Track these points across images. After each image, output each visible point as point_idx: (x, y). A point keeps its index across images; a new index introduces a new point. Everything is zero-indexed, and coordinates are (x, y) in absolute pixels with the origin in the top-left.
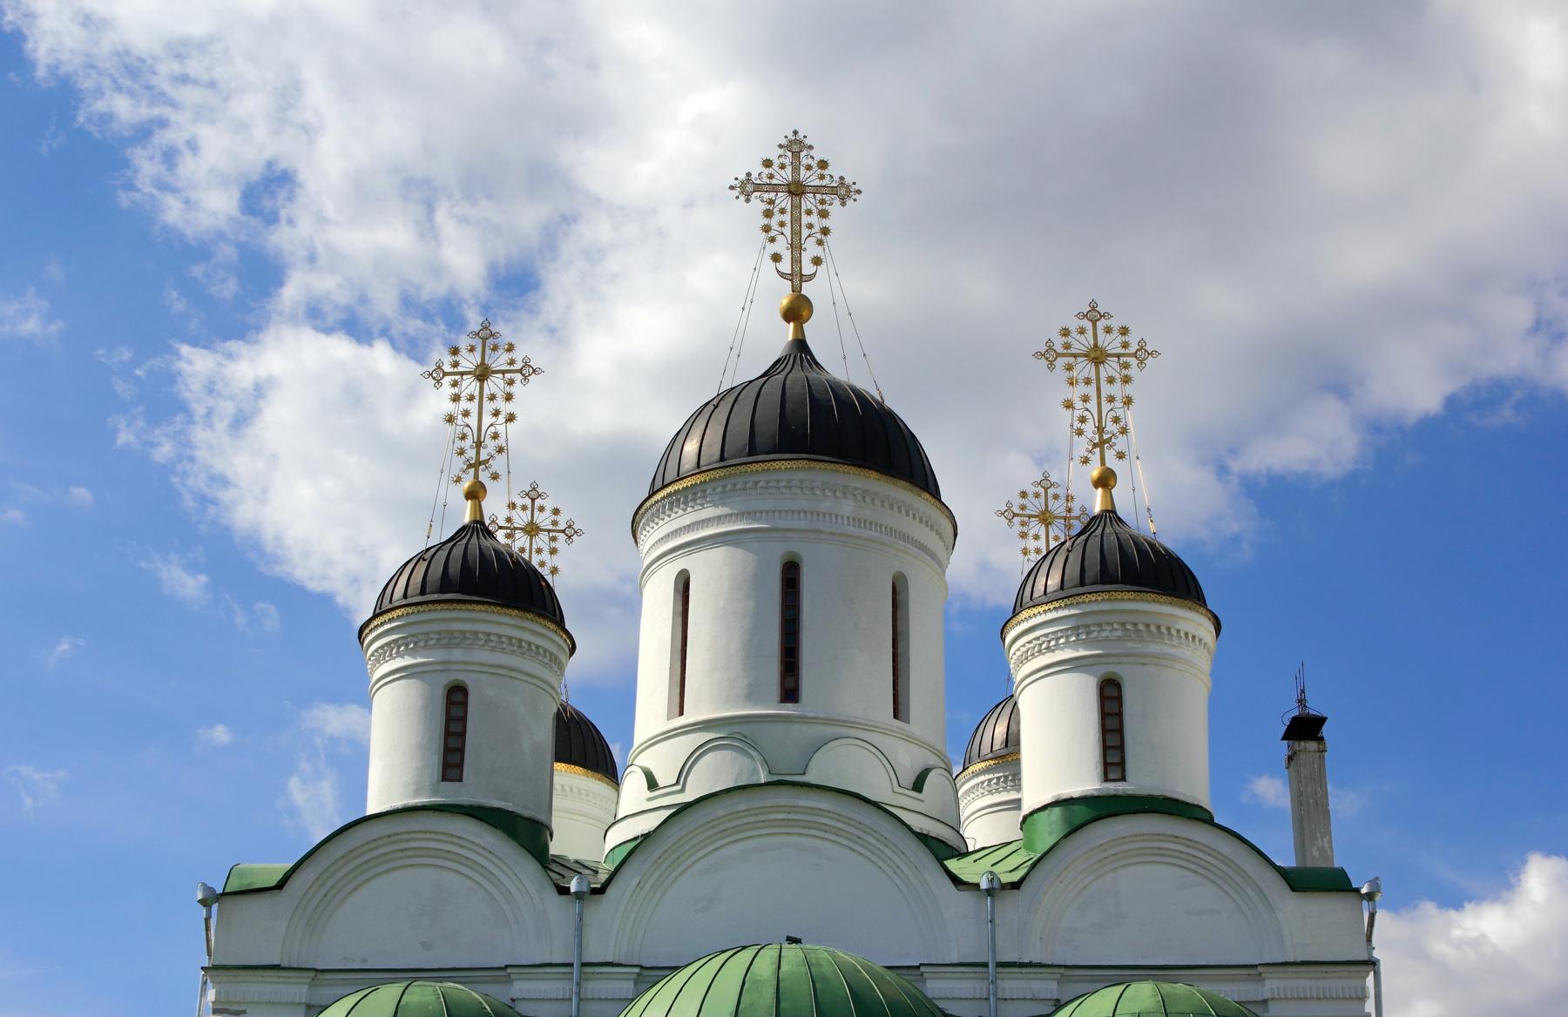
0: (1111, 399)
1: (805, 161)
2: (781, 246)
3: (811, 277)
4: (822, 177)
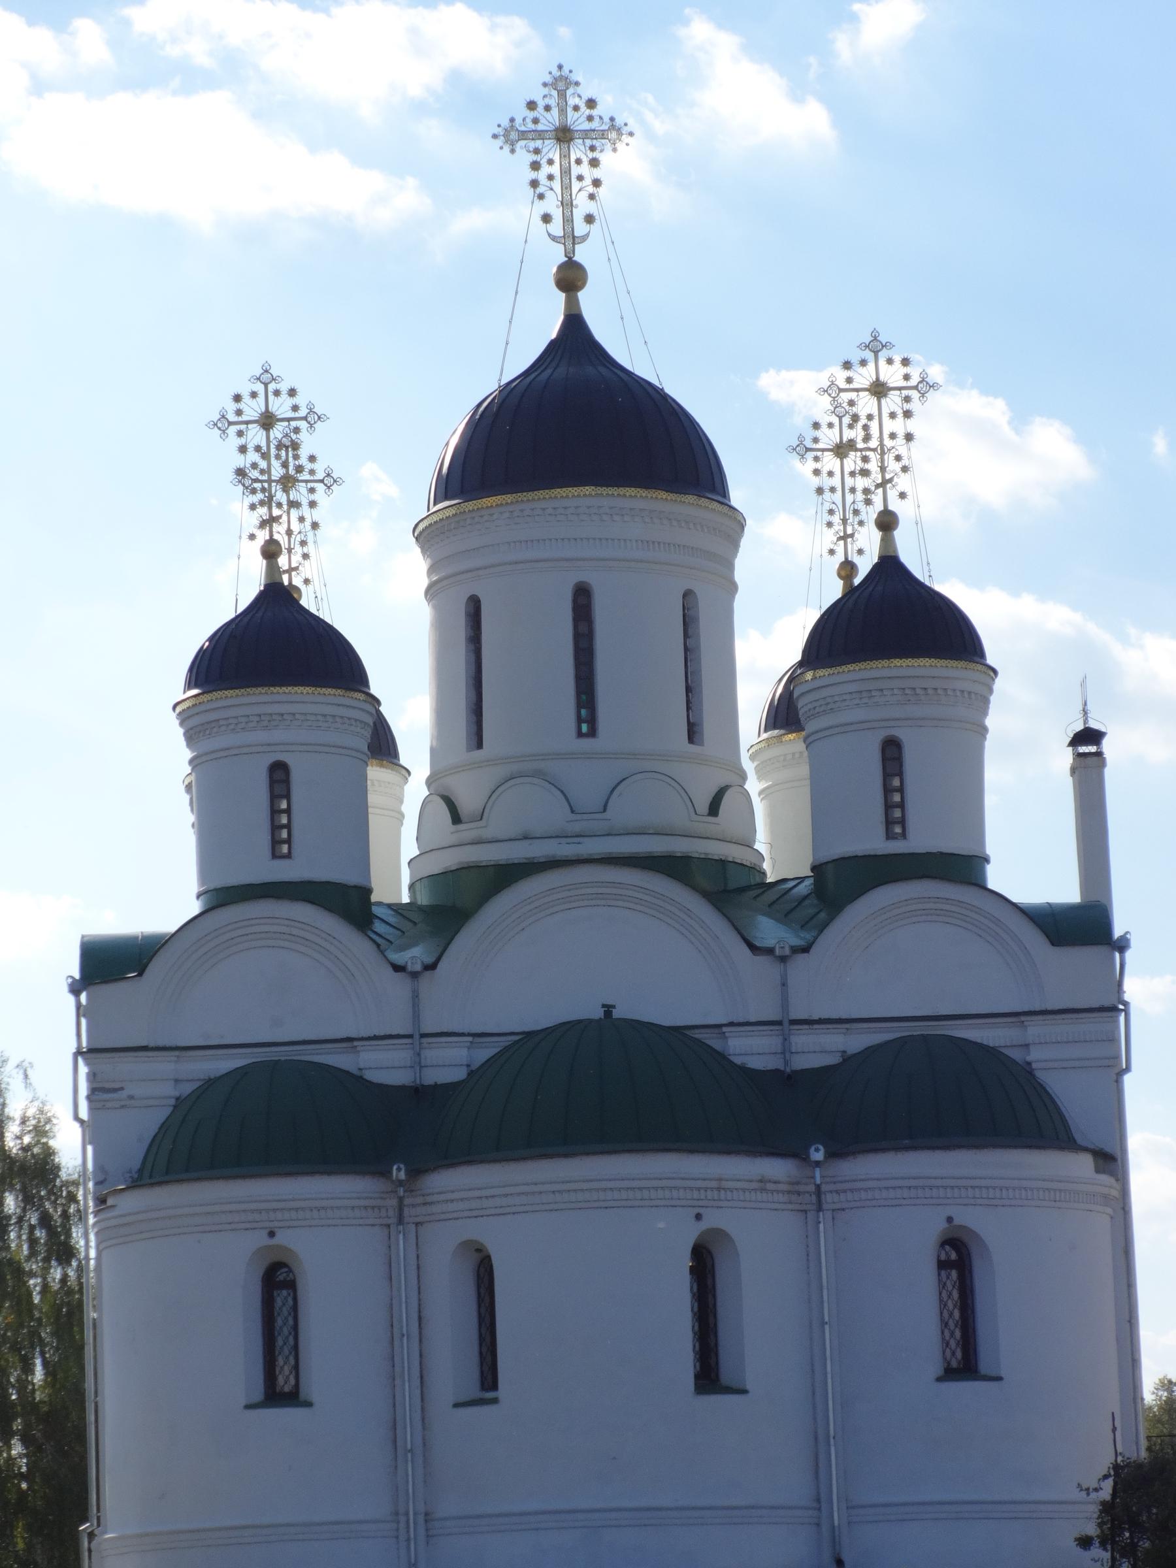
0: (893, 436)
1: (572, 101)
2: (552, 205)
3: (584, 238)
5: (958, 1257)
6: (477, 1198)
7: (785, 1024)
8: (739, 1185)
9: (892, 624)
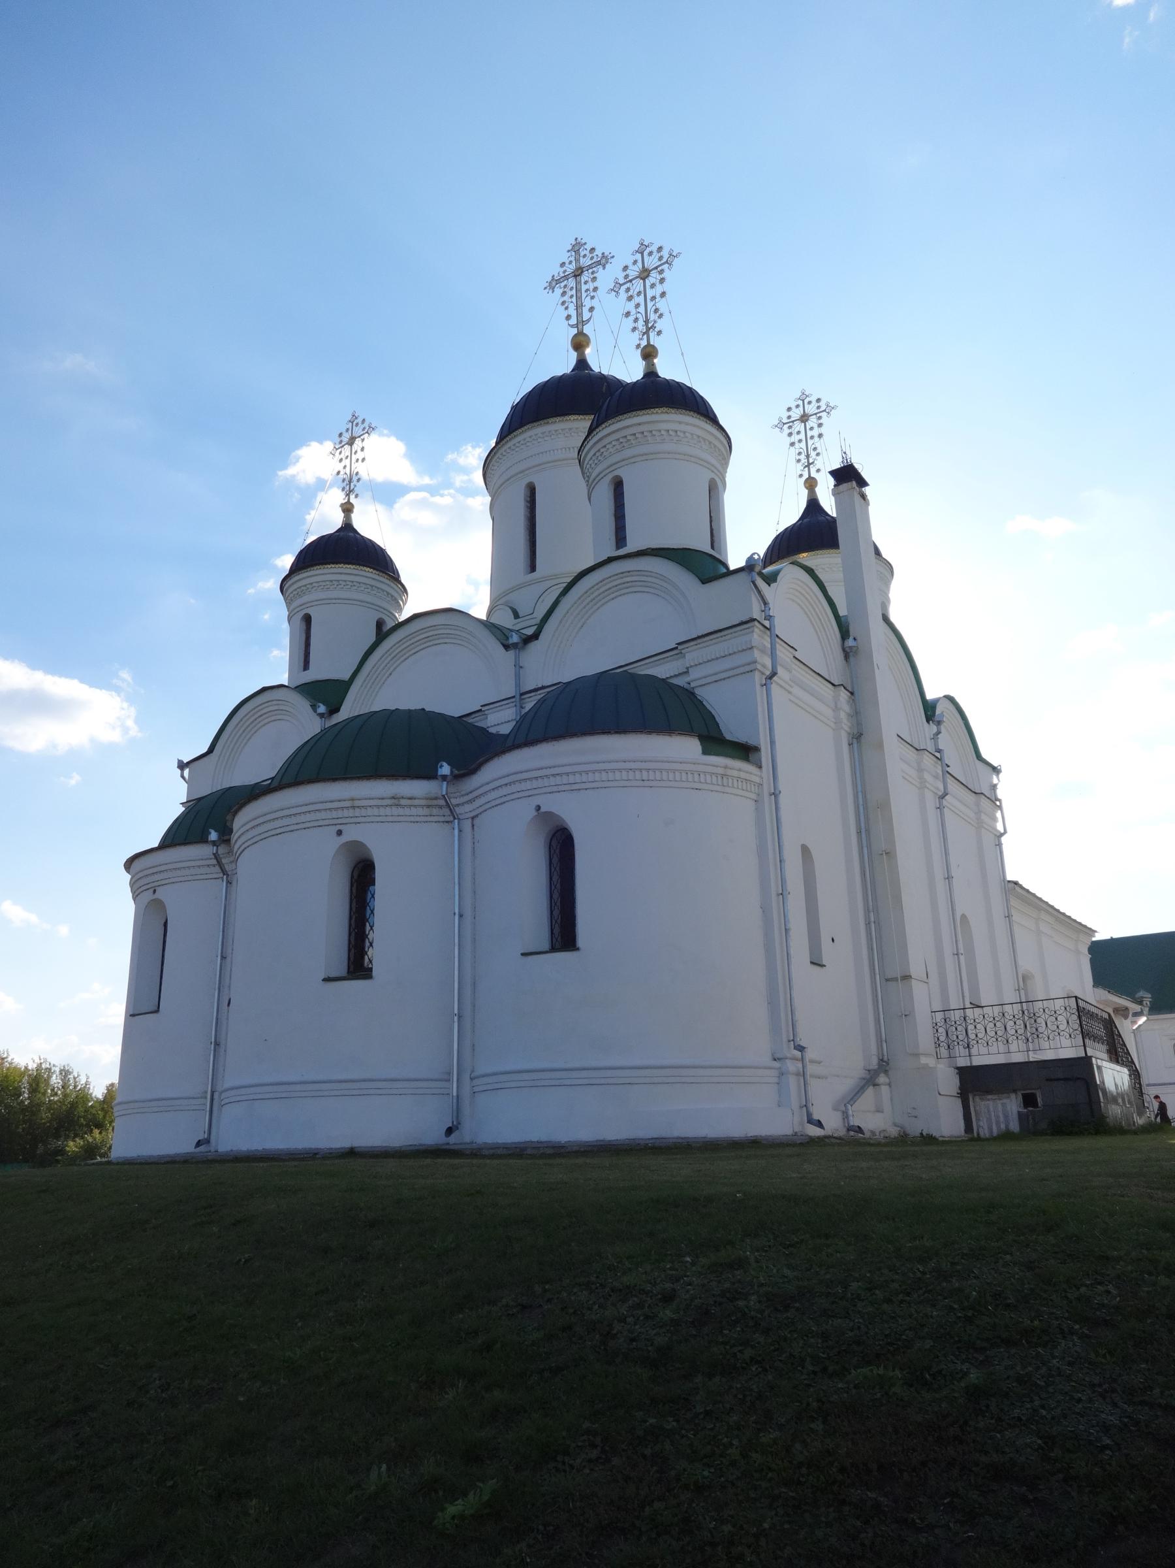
1: (582, 254)
2: (572, 311)
4: (592, 258)
8: (372, 803)
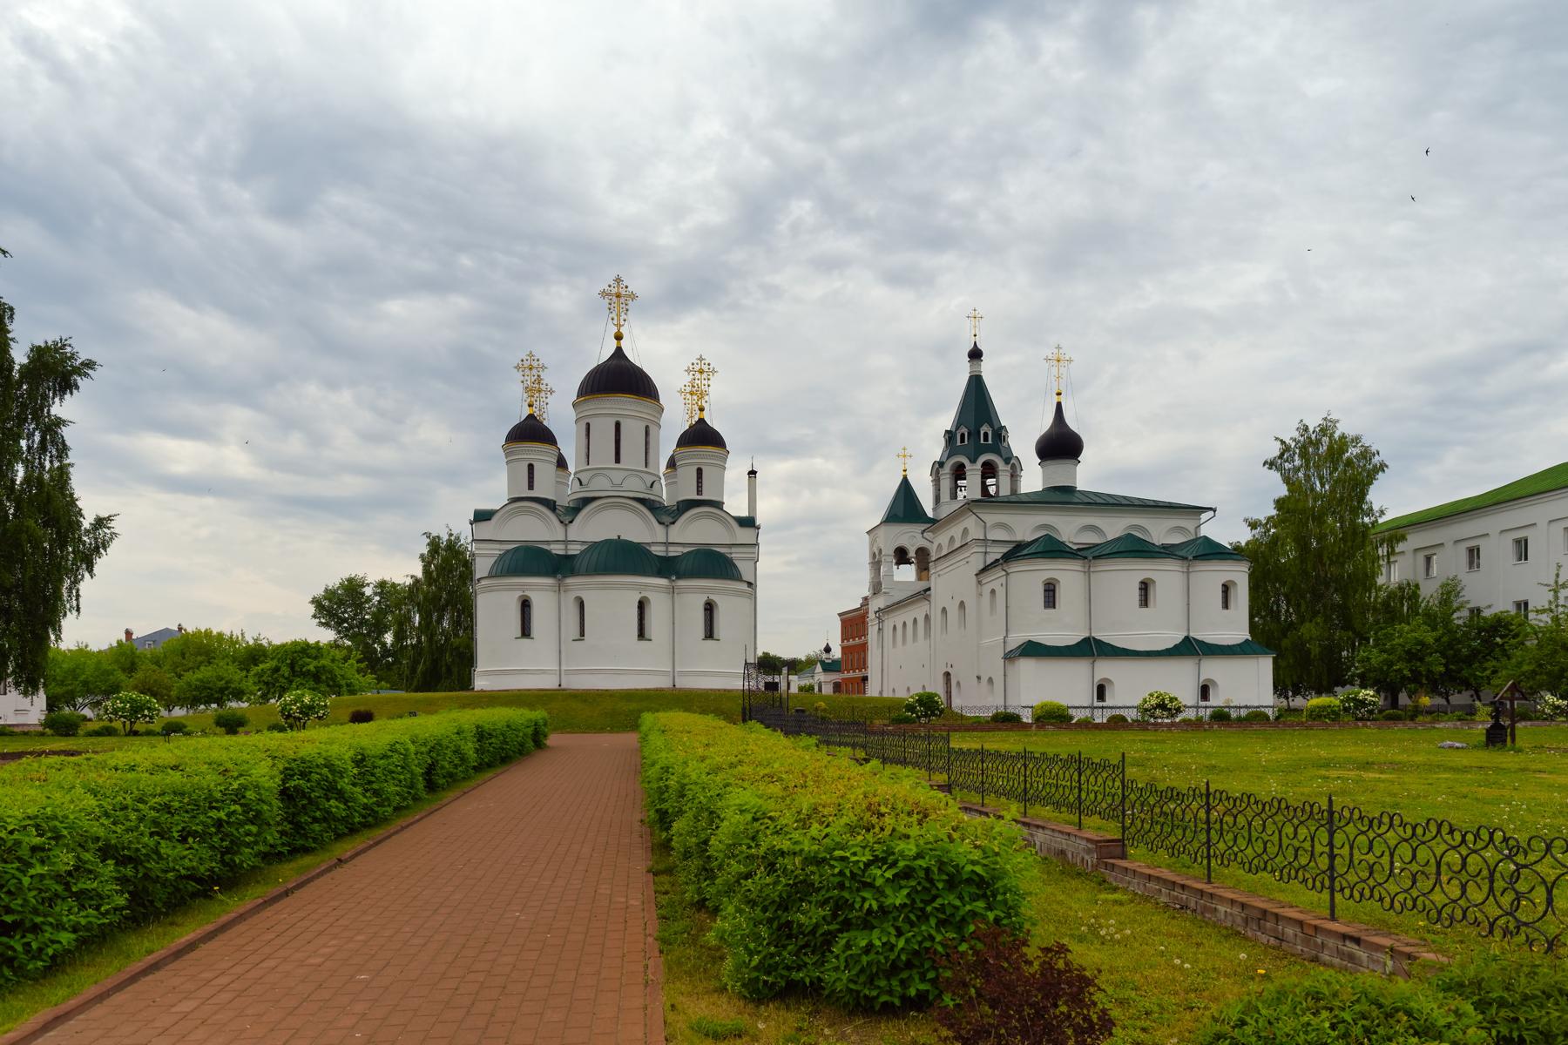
5: (710, 608)
6: (578, 585)
7: (667, 544)
9: (702, 436)
